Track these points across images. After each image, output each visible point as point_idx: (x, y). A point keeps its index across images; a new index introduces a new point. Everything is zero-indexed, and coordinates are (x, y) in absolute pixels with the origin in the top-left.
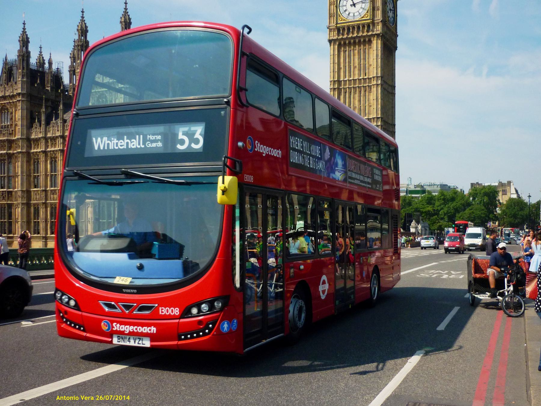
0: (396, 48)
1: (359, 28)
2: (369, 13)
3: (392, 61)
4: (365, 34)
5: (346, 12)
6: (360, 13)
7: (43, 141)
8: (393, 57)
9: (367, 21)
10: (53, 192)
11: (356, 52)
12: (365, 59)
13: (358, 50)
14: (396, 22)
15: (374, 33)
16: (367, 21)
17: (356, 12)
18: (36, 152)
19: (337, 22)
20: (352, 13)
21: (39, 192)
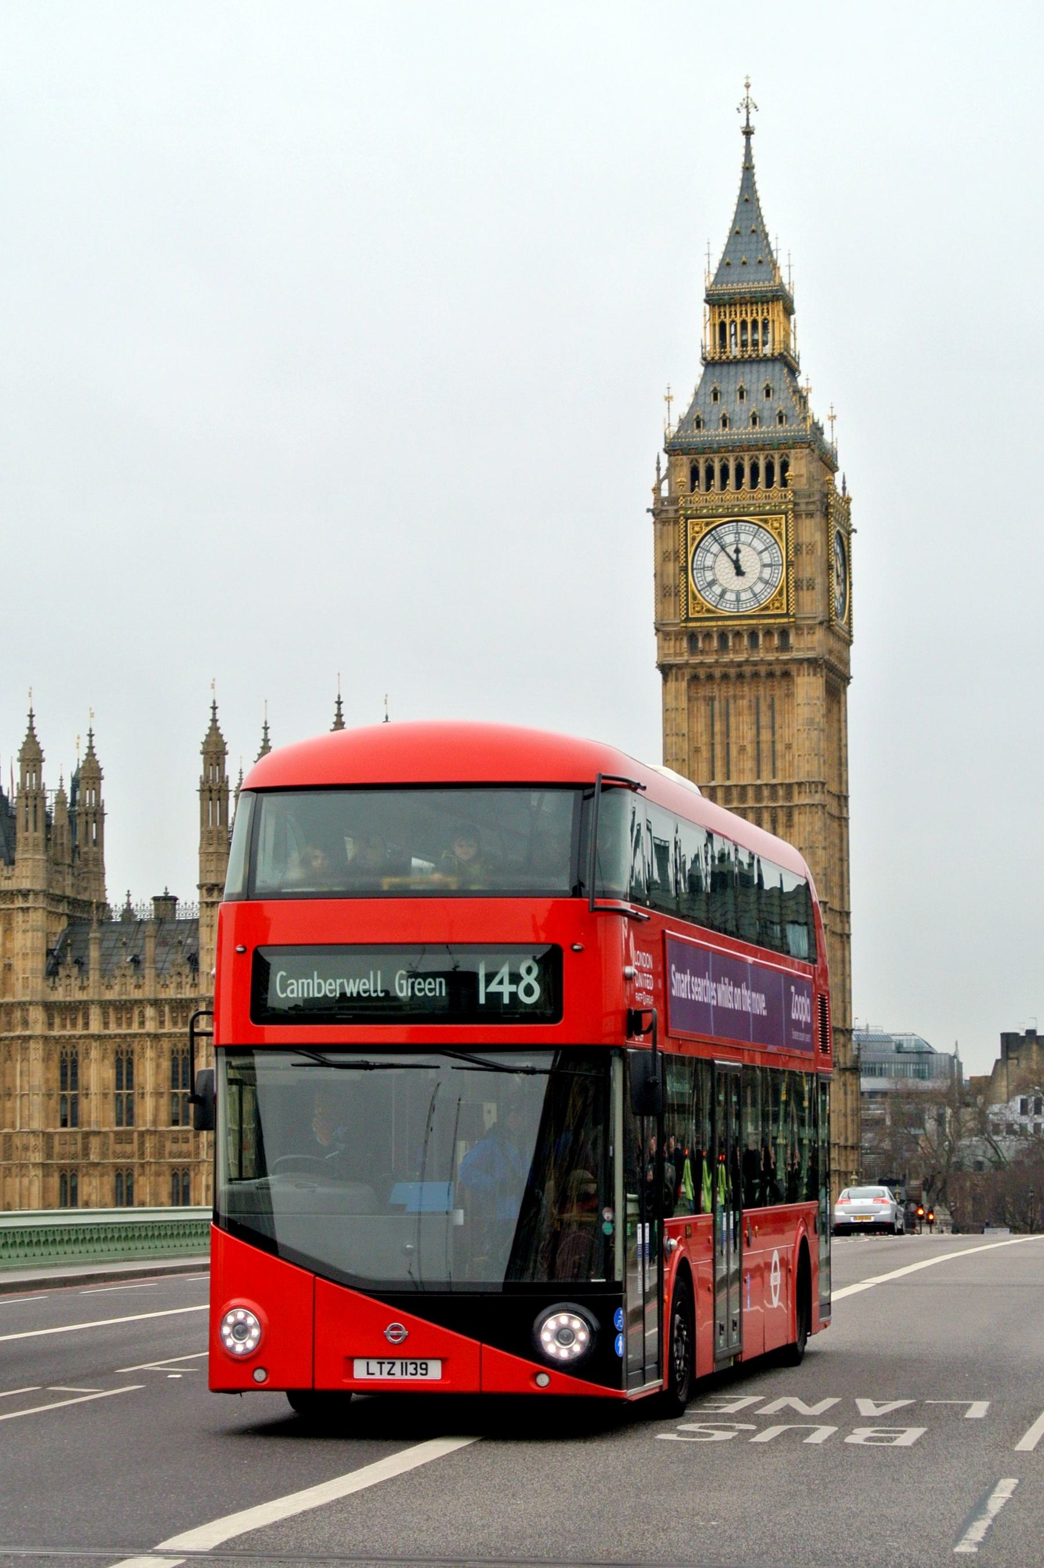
0: (846, 679)
1: (753, 635)
2: (785, 596)
3: (839, 721)
4: (770, 657)
6: (755, 595)
7: (95, 1013)
8: (840, 709)
10: (122, 1138)
11: (745, 703)
12: (773, 728)
13: (750, 701)
14: (850, 610)
15: (800, 655)
16: (778, 621)
17: (745, 590)
18: (71, 1037)
20: (732, 591)
21: (79, 1138)
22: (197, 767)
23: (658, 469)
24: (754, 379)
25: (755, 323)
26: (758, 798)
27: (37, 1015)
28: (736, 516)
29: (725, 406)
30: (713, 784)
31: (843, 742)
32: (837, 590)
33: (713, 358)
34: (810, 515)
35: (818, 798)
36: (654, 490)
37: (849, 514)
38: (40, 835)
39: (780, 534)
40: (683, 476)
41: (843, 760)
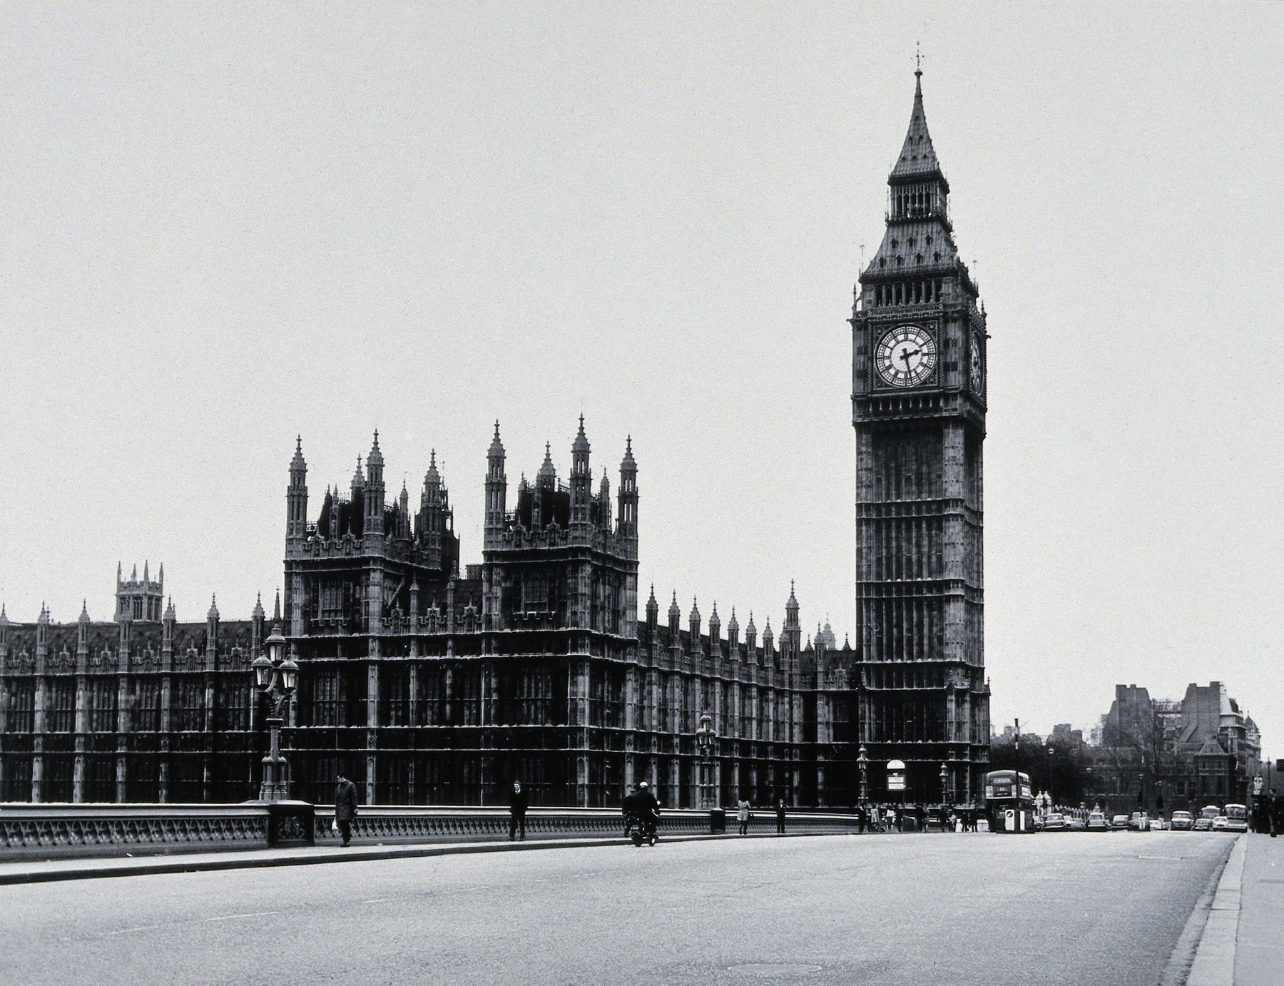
0: (983, 436)
5: (890, 371)
9: (932, 391)
16: (932, 391)
19: (872, 388)
22: (484, 467)
23: (855, 293)
24: (922, 232)
25: (921, 196)
26: (919, 512)
27: (375, 645)
28: (906, 322)
29: (902, 250)
30: (889, 501)
31: (980, 476)
32: (975, 372)
33: (892, 220)
34: (955, 320)
35: (959, 510)
36: (852, 308)
37: (985, 324)
38: (380, 518)
39: (934, 333)
40: (871, 296)
41: (980, 488)
